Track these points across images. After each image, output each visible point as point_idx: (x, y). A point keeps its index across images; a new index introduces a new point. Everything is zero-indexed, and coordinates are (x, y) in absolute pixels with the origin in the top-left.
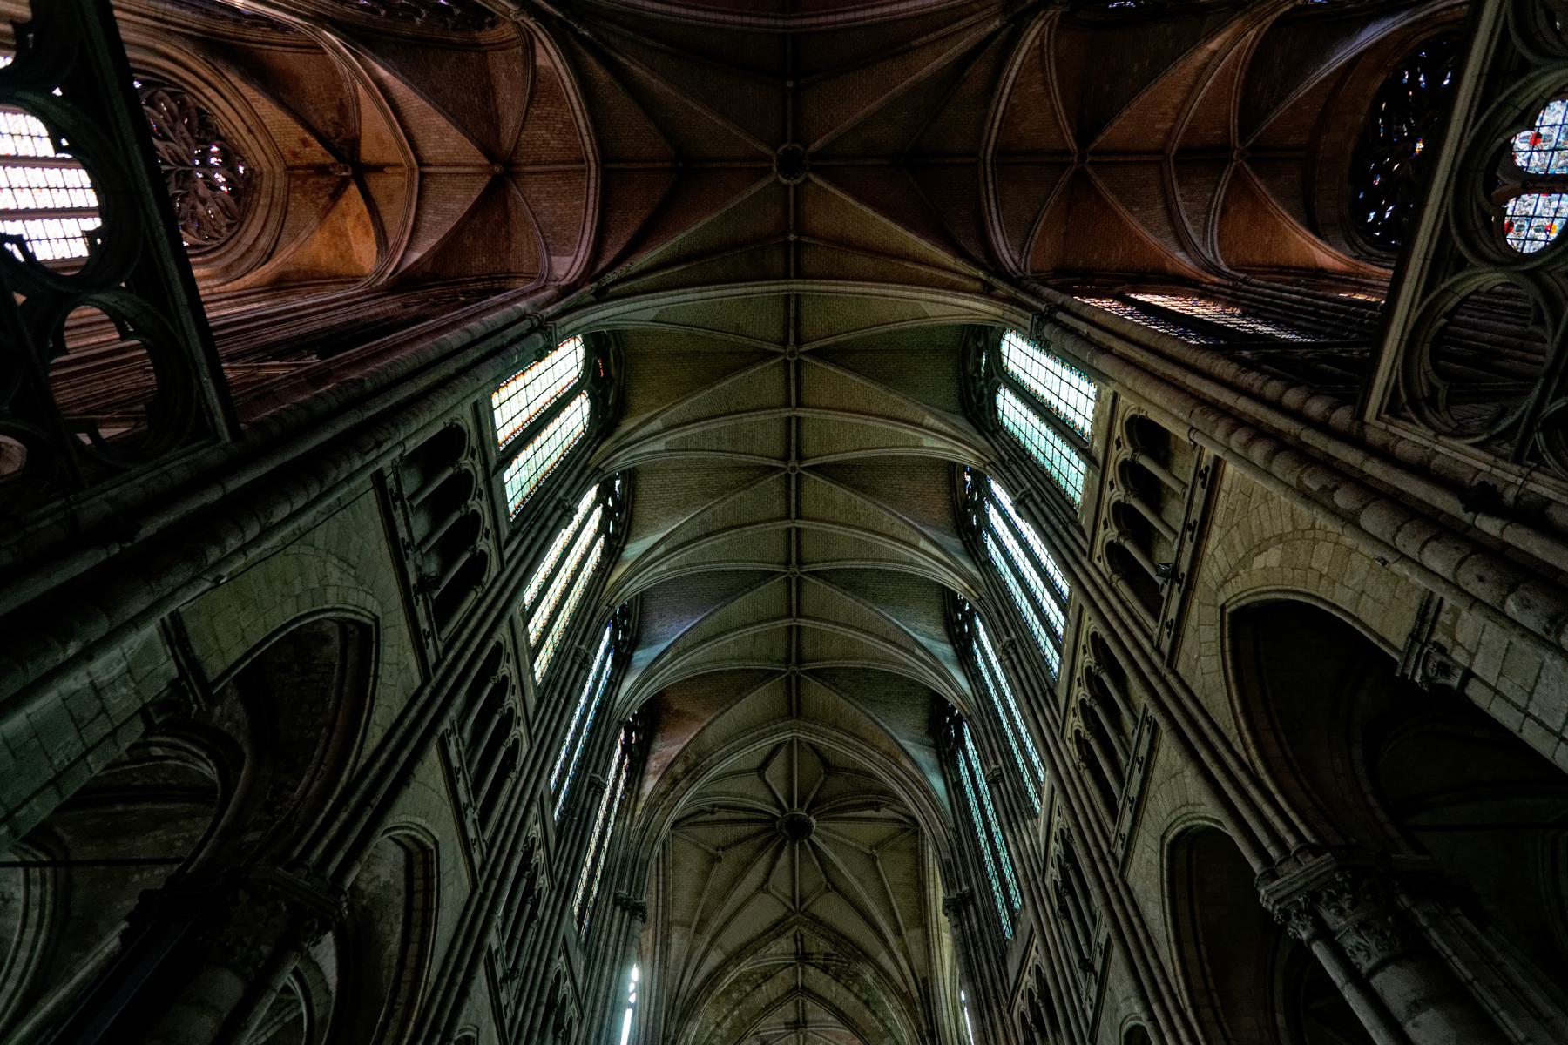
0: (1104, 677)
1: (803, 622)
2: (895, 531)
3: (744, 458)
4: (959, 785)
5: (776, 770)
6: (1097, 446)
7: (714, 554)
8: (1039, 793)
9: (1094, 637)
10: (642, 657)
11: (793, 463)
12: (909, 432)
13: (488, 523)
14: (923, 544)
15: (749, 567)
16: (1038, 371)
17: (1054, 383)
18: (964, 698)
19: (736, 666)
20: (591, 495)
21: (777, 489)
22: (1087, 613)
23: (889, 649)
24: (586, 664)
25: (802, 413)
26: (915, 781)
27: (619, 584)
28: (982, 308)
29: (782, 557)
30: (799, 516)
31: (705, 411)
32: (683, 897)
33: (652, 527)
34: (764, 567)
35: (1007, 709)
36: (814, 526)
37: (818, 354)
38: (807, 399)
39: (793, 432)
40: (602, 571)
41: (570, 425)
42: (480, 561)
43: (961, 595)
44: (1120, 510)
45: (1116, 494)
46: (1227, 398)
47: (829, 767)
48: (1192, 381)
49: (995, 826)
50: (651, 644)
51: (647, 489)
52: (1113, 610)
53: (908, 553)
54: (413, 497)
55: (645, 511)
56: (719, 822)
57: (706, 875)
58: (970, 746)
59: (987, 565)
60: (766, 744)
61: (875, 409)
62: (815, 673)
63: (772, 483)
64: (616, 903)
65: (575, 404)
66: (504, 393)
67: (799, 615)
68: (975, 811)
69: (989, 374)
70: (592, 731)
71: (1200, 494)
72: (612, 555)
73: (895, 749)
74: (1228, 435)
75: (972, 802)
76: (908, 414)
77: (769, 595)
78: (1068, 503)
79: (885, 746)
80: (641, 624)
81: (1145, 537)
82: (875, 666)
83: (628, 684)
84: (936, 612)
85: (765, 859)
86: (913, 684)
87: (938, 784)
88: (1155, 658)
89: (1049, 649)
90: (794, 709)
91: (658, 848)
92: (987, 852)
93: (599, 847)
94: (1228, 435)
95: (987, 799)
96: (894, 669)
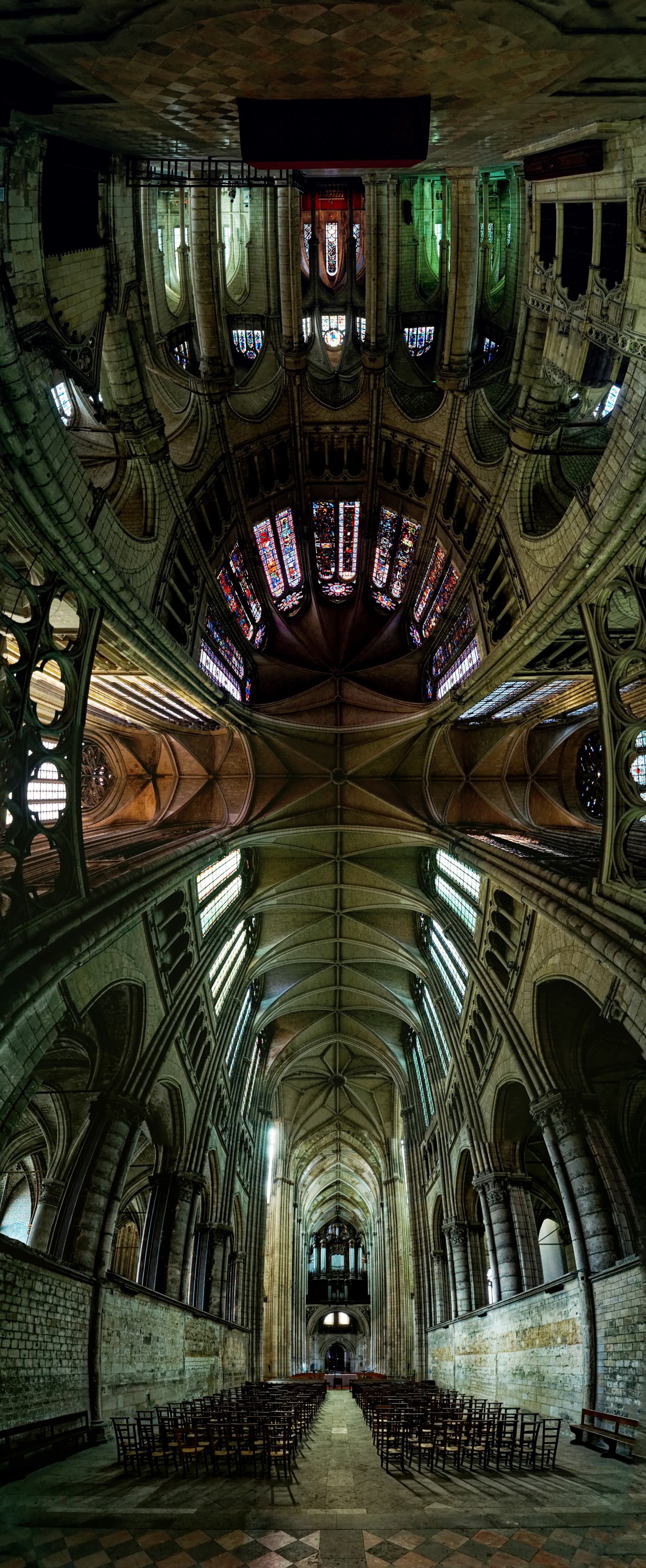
0: (481, 1015)
1: (342, 988)
2: (388, 944)
3: (315, 908)
4: (412, 1064)
5: (328, 1057)
6: (482, 904)
7: (299, 954)
8: (447, 1068)
9: (478, 997)
10: (265, 1004)
11: (338, 911)
12: (394, 896)
13: (193, 938)
14: (401, 951)
15: (316, 961)
16: (453, 868)
17: (461, 874)
18: (417, 1024)
19: (310, 1008)
20: (241, 925)
21: (330, 923)
22: (476, 985)
23: (383, 1001)
24: (239, 1007)
25: (343, 887)
26: (393, 1062)
27: (254, 969)
28: (426, 839)
29: (332, 956)
30: (341, 937)
31: (296, 885)
32: (288, 1109)
33: (270, 941)
34: (323, 961)
35: (437, 1030)
36: (349, 941)
37: (351, 859)
38: (346, 880)
39: (338, 895)
40: (246, 962)
41: (232, 892)
42: (189, 956)
43: (418, 976)
44: (493, 936)
45: (490, 928)
46: (536, 882)
47: (353, 1055)
48: (521, 874)
49: (426, 1081)
50: (269, 997)
51: (268, 922)
52: (487, 984)
53: (393, 955)
54: (159, 925)
55: (266, 933)
56: (303, 1078)
57: (297, 1100)
58: (418, 1046)
59: (430, 961)
60: (324, 1045)
61: (377, 885)
62: (347, 1012)
63: (328, 920)
64: (259, 1110)
65: (235, 881)
66: (203, 875)
67: (340, 984)
68: (419, 1075)
69: (432, 870)
70: (243, 1038)
71: (527, 927)
72: (250, 954)
73: (384, 1048)
74: (538, 900)
75: (418, 1071)
76: (394, 888)
77: (326, 974)
78: (469, 932)
79: (379, 1046)
80: (264, 988)
81: (502, 948)
82: (376, 1009)
83: (259, 1016)
84: (406, 984)
85: (323, 1094)
86: (394, 1017)
87: (403, 1063)
88: (504, 1007)
89: (457, 1002)
90: (337, 1029)
91: (276, 1089)
92: (422, 1092)
93: (250, 1088)
94: (538, 900)
95: (424, 1070)
96: (385, 1011)
